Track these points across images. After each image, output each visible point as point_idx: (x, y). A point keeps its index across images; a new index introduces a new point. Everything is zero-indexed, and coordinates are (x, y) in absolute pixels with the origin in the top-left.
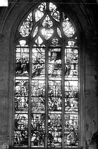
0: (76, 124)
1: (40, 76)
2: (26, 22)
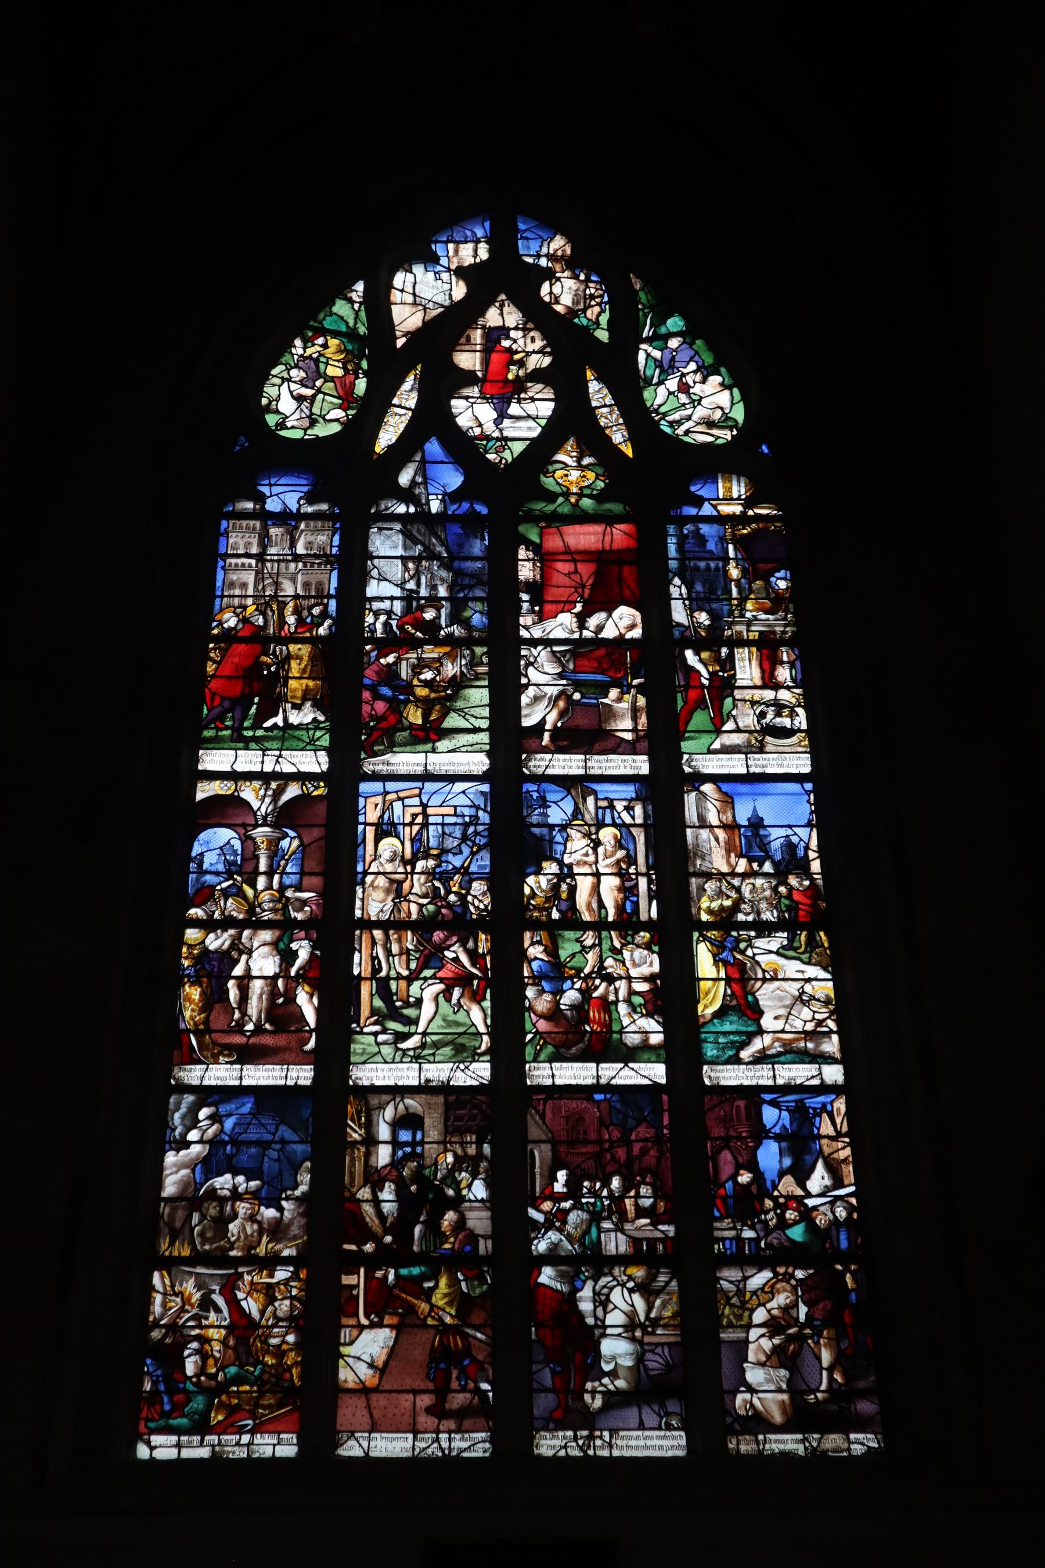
0: (838, 1182)
1: (443, 745)
2: (320, 341)
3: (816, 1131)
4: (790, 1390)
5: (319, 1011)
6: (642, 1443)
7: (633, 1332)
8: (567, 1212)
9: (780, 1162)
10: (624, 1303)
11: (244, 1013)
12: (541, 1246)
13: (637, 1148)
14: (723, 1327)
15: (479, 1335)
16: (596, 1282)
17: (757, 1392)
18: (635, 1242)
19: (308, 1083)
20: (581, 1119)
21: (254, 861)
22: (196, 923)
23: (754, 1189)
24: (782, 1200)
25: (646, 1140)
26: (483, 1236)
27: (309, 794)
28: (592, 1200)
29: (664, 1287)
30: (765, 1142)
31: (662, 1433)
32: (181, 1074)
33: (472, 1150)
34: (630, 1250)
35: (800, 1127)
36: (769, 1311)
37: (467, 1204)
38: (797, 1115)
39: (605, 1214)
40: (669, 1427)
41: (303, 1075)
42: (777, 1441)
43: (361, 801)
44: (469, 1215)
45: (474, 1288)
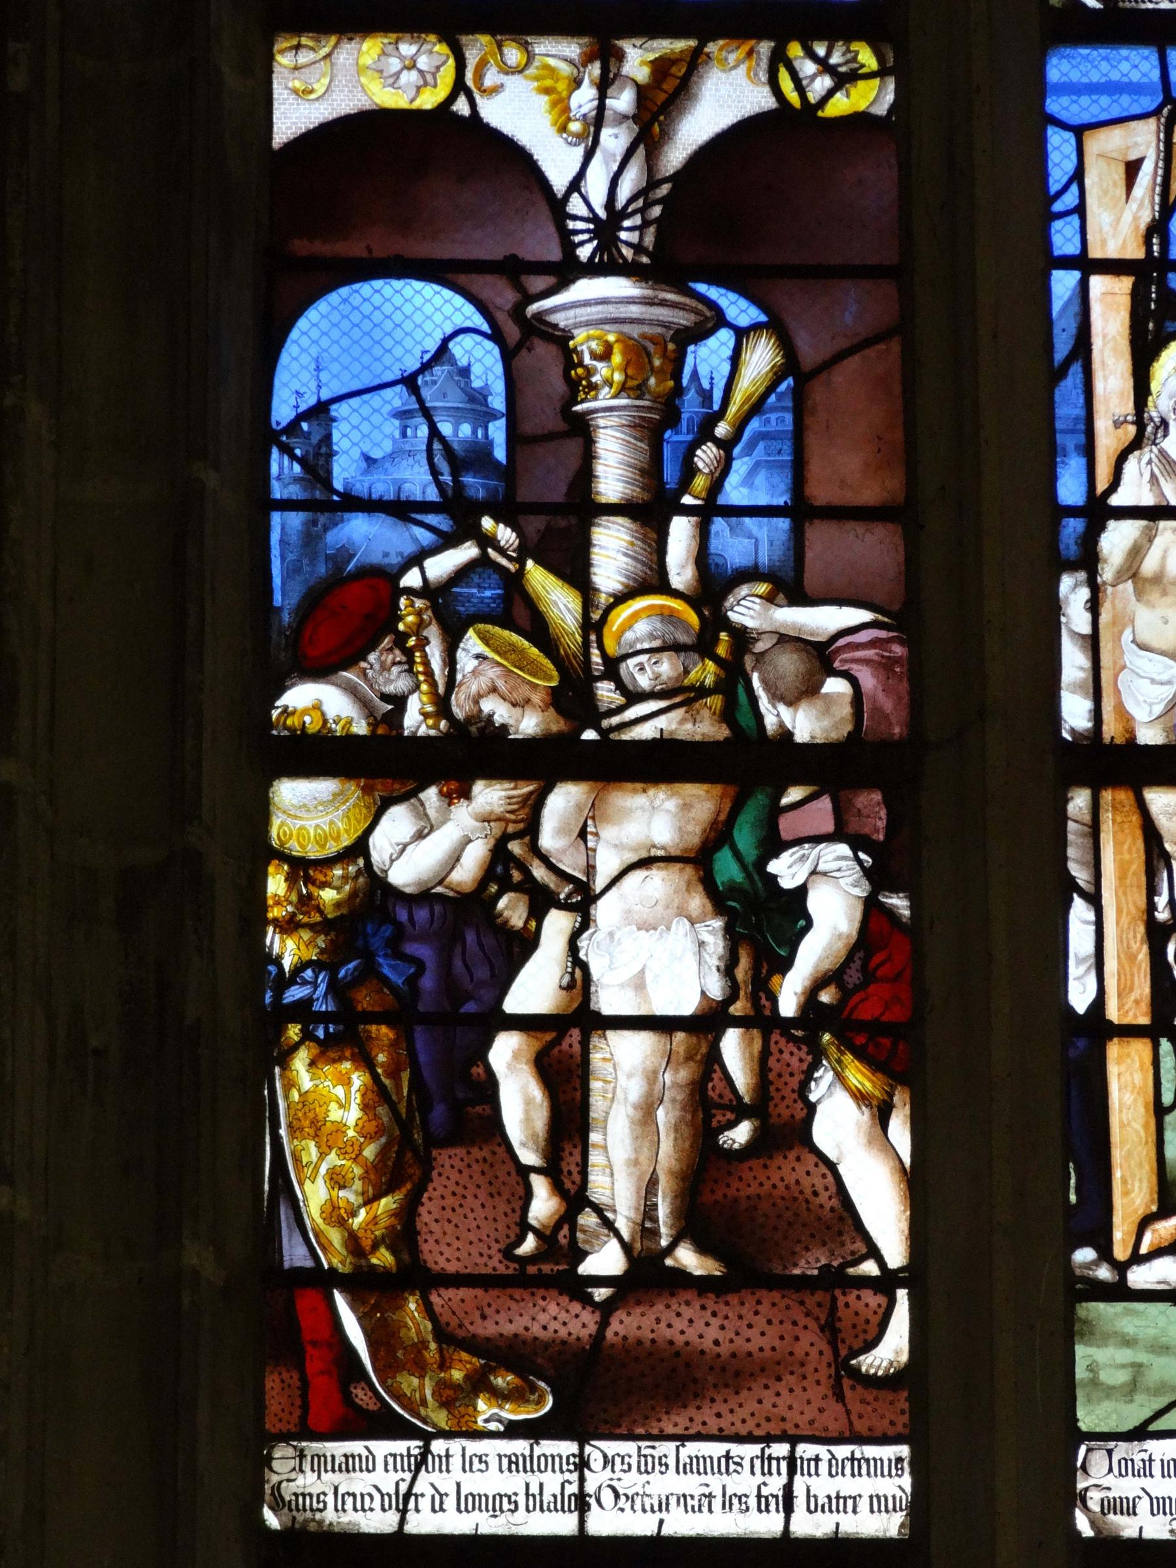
5: (917, 1183)
11: (575, 1198)
19: (890, 1525)
21: (573, 447)
22: (317, 753)
27: (810, 109)
32: (307, 1481)
41: (863, 1493)
43: (1059, 143)
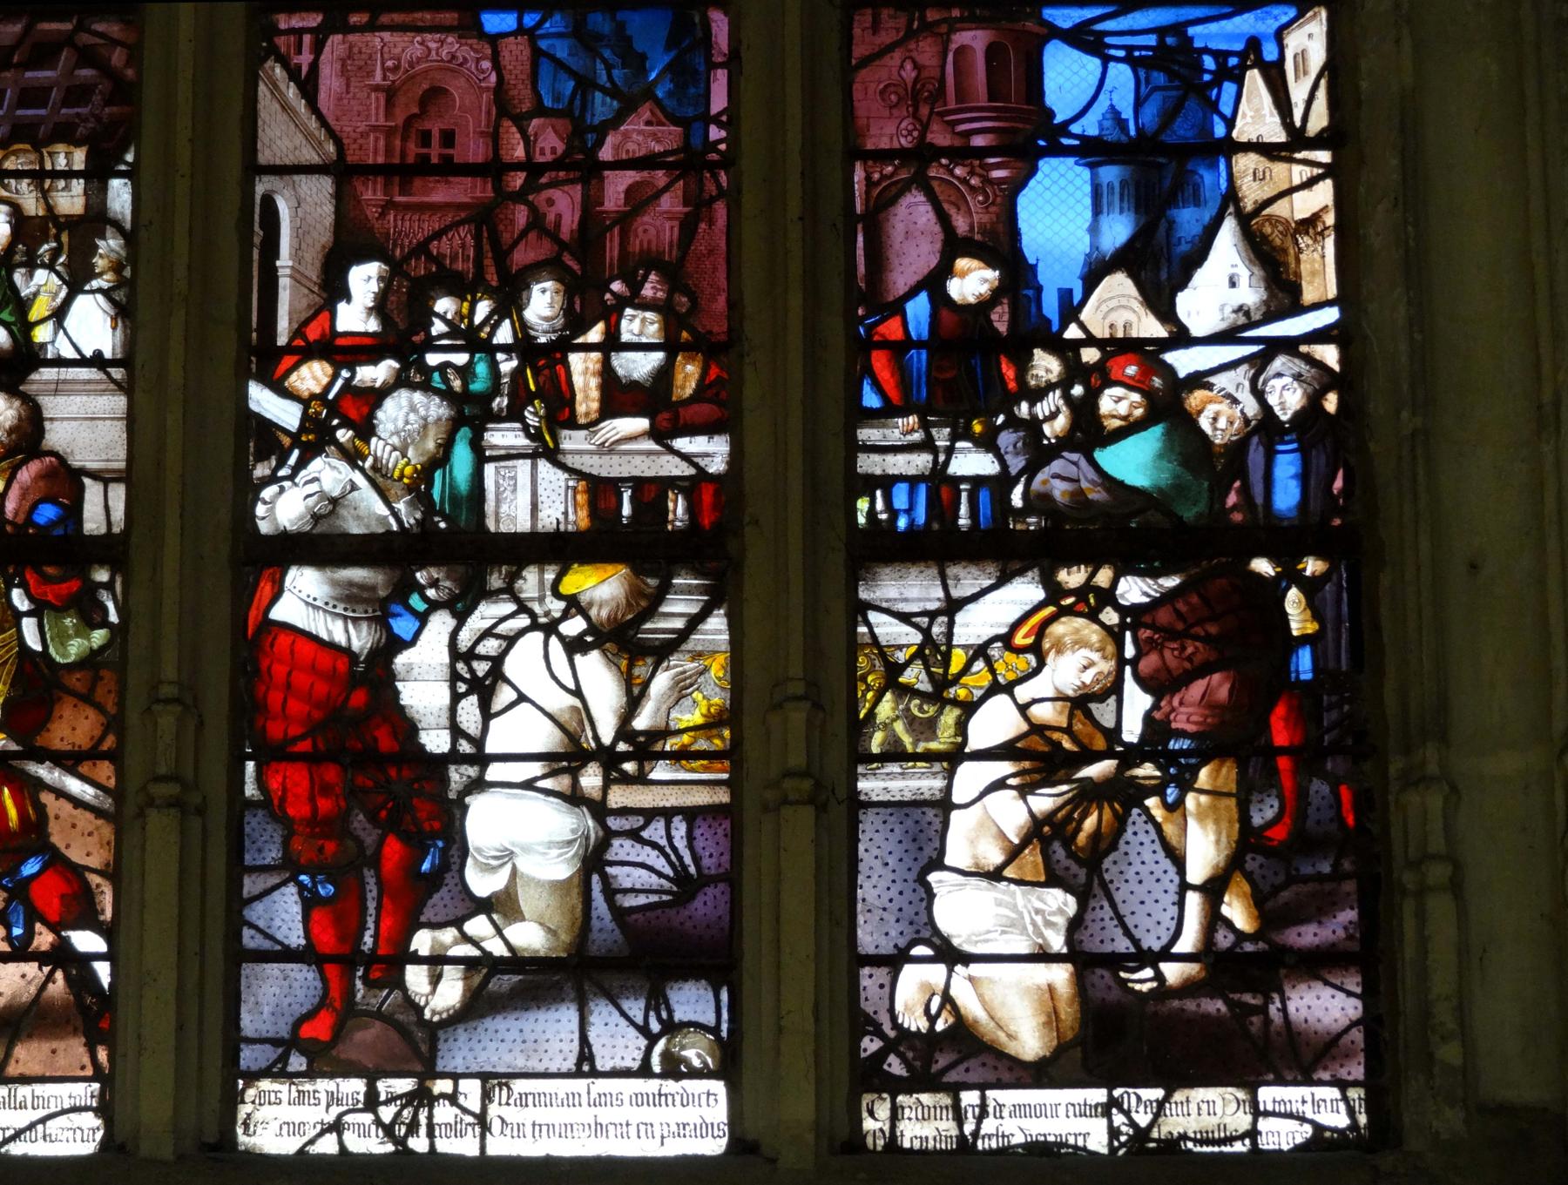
0: (1284, 294)
3: (1220, 130)
4: (1079, 957)
6: (584, 1114)
7: (575, 774)
8: (376, 396)
9: (1094, 230)
10: (551, 686)
12: (285, 507)
13: (617, 186)
14: (870, 758)
15: (74, 786)
16: (461, 618)
17: (968, 959)
18: (599, 490)
20: (434, 96)
23: (1000, 320)
24: (1090, 355)
25: (647, 162)
26: (95, 475)
28: (461, 359)
29: (684, 635)
30: (1047, 166)
31: (652, 1085)
33: (71, 200)
34: (580, 519)
35: (1169, 116)
36: (1023, 709)
37: (48, 374)
38: (1160, 78)
39: (501, 402)
40: (674, 1069)
42: (1019, 1110)
44: (52, 406)
45: (63, 638)
